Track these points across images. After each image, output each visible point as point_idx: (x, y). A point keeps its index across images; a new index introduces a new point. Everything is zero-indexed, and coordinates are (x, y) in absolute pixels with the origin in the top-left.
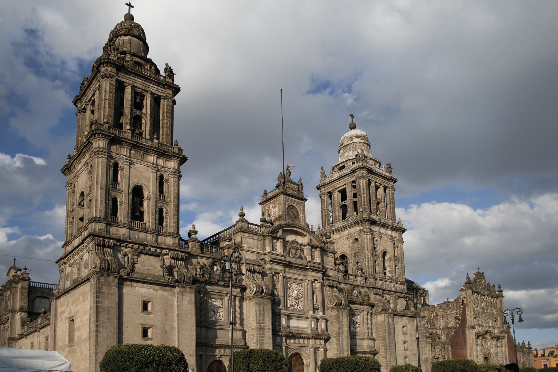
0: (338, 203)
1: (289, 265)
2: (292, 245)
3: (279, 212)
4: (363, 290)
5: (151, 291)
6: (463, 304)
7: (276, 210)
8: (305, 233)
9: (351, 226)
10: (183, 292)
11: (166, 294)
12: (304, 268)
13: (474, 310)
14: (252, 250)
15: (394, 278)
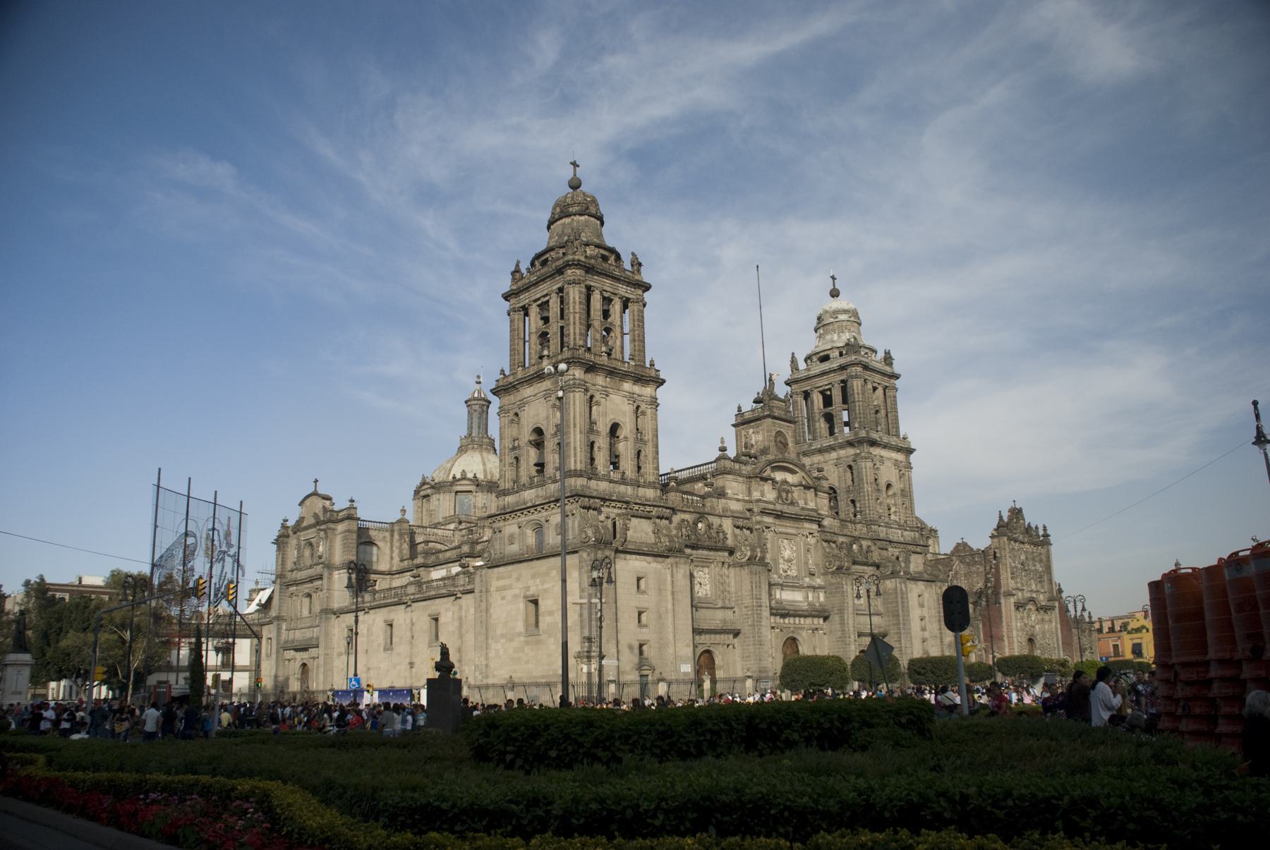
0: (819, 409)
1: (779, 516)
2: (783, 487)
3: (764, 441)
4: (865, 543)
5: (645, 563)
6: (995, 557)
7: (760, 437)
8: (796, 469)
9: (841, 447)
10: (677, 563)
11: (659, 566)
12: (796, 518)
13: (1011, 567)
14: (736, 497)
15: (902, 522)
